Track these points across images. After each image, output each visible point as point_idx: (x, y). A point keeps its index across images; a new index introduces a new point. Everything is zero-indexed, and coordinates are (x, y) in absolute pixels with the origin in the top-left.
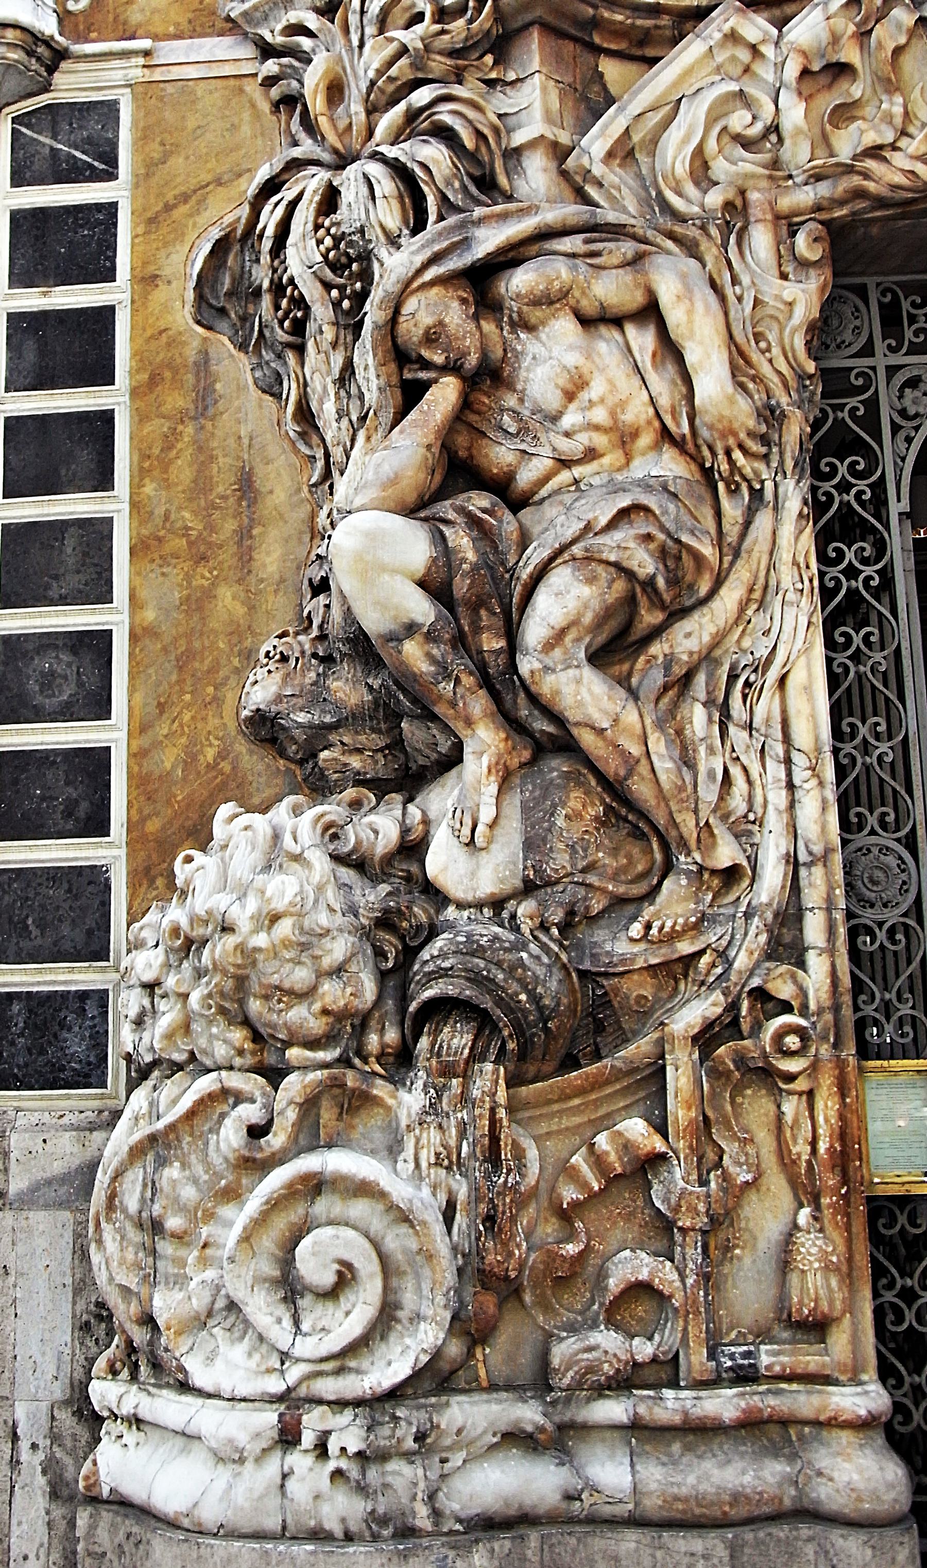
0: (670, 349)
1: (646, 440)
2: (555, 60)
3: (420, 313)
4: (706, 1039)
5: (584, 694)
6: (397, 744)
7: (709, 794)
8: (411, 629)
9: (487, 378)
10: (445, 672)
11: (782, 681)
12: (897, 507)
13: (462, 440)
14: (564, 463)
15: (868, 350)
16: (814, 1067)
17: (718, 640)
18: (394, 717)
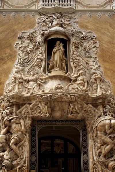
0: (21, 125)
1: (19, 131)
2: (16, 106)
3: (6, 123)
4: (19, 168)
5: (14, 147)
6: (3, 149)
7: (21, 153)
8: (4, 142)
9: (10, 127)
10: (6, 145)
11: (26, 147)
12: (37, 135)
13: (9, 130)
14: (14, 132)
15: (36, 124)
16: (25, 171)
17: (23, 144)
18: (3, 147)
